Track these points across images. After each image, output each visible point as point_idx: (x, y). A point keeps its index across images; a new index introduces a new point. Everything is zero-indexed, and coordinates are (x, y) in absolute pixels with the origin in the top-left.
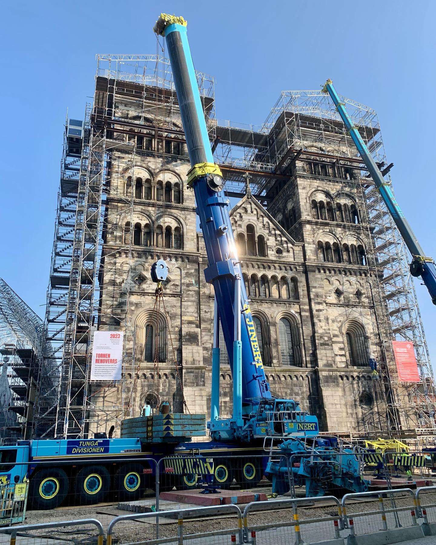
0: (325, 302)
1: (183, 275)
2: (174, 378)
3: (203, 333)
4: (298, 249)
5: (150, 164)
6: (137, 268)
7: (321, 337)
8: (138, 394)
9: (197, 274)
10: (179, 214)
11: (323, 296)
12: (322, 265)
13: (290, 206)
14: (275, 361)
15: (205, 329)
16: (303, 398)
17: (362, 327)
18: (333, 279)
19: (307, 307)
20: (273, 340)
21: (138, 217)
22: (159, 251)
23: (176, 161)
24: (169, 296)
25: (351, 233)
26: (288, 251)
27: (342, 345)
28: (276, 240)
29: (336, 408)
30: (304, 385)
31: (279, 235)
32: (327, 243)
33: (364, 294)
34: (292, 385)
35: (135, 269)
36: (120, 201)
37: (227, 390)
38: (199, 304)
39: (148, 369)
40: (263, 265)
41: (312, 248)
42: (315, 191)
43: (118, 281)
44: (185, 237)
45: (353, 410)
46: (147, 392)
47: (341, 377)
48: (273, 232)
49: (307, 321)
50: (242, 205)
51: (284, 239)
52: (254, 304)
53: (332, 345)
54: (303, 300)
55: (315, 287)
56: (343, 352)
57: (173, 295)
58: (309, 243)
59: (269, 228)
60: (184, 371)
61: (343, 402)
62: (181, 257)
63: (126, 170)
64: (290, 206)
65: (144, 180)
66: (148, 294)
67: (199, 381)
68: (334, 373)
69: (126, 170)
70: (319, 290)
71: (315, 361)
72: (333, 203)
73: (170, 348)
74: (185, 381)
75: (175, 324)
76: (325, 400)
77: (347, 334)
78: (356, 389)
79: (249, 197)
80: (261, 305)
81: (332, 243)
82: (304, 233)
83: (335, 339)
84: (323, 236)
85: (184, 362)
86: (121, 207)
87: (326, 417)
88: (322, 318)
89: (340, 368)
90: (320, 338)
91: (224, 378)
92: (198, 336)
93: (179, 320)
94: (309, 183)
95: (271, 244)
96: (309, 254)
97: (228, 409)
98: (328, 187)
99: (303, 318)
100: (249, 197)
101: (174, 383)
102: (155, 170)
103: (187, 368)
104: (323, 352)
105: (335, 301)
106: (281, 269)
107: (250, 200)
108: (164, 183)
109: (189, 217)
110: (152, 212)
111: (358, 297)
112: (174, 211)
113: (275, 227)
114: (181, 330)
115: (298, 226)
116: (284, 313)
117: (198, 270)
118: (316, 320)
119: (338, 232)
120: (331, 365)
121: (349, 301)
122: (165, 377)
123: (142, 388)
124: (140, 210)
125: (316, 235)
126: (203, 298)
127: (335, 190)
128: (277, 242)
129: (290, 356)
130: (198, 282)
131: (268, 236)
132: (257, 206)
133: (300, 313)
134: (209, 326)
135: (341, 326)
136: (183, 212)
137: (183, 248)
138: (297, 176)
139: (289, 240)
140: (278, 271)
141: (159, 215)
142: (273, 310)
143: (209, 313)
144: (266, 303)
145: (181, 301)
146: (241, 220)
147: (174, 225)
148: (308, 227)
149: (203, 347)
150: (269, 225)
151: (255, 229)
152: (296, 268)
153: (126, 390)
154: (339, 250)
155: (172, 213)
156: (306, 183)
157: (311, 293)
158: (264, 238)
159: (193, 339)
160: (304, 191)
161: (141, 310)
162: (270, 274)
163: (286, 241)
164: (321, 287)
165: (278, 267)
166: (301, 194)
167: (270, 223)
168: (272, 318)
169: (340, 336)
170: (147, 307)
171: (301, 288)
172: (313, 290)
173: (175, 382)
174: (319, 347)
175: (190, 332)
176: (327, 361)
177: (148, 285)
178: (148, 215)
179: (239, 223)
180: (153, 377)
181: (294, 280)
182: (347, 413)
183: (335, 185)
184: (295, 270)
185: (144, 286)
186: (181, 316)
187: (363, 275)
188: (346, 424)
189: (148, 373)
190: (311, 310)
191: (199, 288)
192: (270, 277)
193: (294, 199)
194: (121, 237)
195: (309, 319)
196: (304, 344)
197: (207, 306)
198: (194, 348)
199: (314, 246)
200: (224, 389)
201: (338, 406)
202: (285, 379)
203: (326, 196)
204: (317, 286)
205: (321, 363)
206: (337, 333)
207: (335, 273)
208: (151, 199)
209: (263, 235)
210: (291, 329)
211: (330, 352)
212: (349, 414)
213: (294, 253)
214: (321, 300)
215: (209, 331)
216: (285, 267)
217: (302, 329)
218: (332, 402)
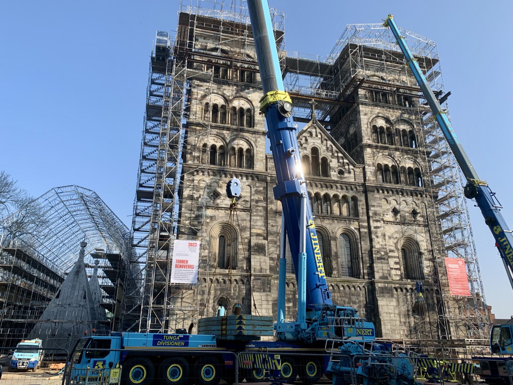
0: (383, 220)
1: (253, 192)
2: (243, 283)
3: (270, 245)
4: (358, 171)
5: (225, 92)
6: (212, 185)
7: (378, 252)
8: (212, 297)
9: (265, 191)
10: (250, 137)
11: (381, 214)
12: (381, 186)
13: (352, 131)
14: (335, 272)
15: (272, 241)
16: (360, 307)
17: (417, 244)
18: (390, 199)
19: (366, 224)
20: (333, 253)
21: (213, 140)
22: (232, 170)
23: (248, 89)
24: (240, 211)
25: (409, 156)
26: (350, 172)
27: (397, 260)
28: (338, 162)
29: (390, 317)
30: (361, 295)
31: (342, 157)
33: (419, 213)
34: (350, 294)
35: (210, 186)
36: (198, 125)
37: (291, 297)
38: (266, 219)
39: (220, 275)
40: (326, 185)
41: (372, 170)
42: (376, 117)
43: (195, 196)
44: (255, 158)
45: (406, 319)
46: (220, 295)
47: (396, 289)
48: (336, 155)
49: (365, 237)
50: (307, 129)
51: (346, 161)
52: (317, 220)
53: (388, 260)
54: (363, 218)
55: (374, 206)
56: (398, 266)
57: (244, 210)
58: (369, 165)
59: (332, 151)
60: (252, 278)
61: (397, 311)
62: (251, 176)
63: (204, 97)
64: (352, 131)
65: (219, 106)
66: (221, 208)
67: (265, 287)
68: (389, 285)
69: (204, 97)
70: (377, 209)
71: (371, 273)
72: (393, 128)
73: (241, 257)
74: (254, 287)
75: (245, 236)
76: (380, 309)
77: (402, 249)
78: (409, 300)
79: (315, 122)
80: (323, 221)
81: (390, 166)
82: (365, 156)
83: (391, 254)
84: (382, 159)
85: (252, 270)
86: (199, 130)
87: (381, 324)
88: (379, 234)
89: (395, 280)
90: (377, 253)
91: (288, 286)
92: (265, 247)
93: (249, 233)
94: (370, 110)
95: (334, 166)
96: (368, 174)
97: (291, 313)
98: (388, 114)
99: (362, 234)
100: (315, 122)
101: (244, 288)
102: (229, 96)
104: (379, 265)
105: (392, 219)
106: (342, 189)
107: (315, 124)
108: (237, 109)
109: (259, 139)
111: (413, 216)
112: (245, 134)
113: (337, 150)
114: (250, 242)
115: (359, 150)
116: (344, 229)
117: (266, 188)
118: (373, 236)
119: (396, 155)
120: (386, 278)
121: (405, 220)
122: (235, 283)
123: (215, 292)
124: (216, 133)
125: (376, 158)
126: (270, 214)
127: (394, 116)
128: (339, 164)
129: (348, 268)
130: (266, 199)
131: (331, 158)
132: (321, 130)
133: (359, 230)
134: (275, 239)
135: (397, 242)
136: (254, 136)
137: (253, 168)
138: (359, 103)
139: (350, 162)
140: (340, 190)
141: (233, 137)
142: (334, 226)
143: (275, 227)
144: (328, 219)
145: (251, 216)
146: (307, 143)
148: (369, 150)
149: (270, 258)
150: (332, 148)
151: (319, 152)
152: (356, 188)
153: (201, 293)
154: (397, 172)
156: (367, 109)
157: (370, 211)
158: (327, 160)
159: (261, 249)
160: (366, 117)
161: (215, 222)
162: (332, 193)
163: (347, 163)
164: (379, 206)
165: (339, 187)
166: (363, 119)
167: (334, 146)
168: (333, 233)
169: (396, 252)
170: (221, 220)
171: (361, 207)
172: (372, 208)
173: (244, 287)
174: (375, 261)
175: (258, 243)
176: (383, 273)
177: (221, 201)
178: (222, 138)
179: (304, 145)
180: (225, 282)
181: (354, 199)
182: (401, 322)
183: (394, 112)
184: (355, 190)
185: (218, 201)
186: (250, 229)
187: (419, 196)
188: (399, 331)
189: (221, 279)
190: (369, 227)
191: (267, 204)
192: (332, 196)
194: (198, 157)
195: (367, 235)
196: (362, 258)
197: (273, 220)
198: (262, 258)
199: (374, 168)
200: (288, 296)
201: (392, 315)
202: (344, 288)
203: (386, 122)
204: (376, 205)
205: (378, 275)
206: (393, 248)
207: (393, 193)
208: (225, 123)
209: (326, 157)
210: (350, 244)
211: (386, 265)
212: (402, 323)
213: (355, 174)
214: (379, 218)
215: (275, 243)
216: (346, 187)
217: (361, 244)
218: (387, 311)
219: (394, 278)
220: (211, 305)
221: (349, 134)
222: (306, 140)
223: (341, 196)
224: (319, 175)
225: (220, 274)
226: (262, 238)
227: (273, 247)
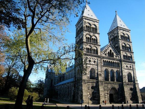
1: (98, 61)
4: (120, 56)
5: (91, 34)
15: (102, 73)
18: (126, 63)
32: (125, 55)
38: (101, 67)
55: (123, 65)
57: (96, 65)
67: (102, 84)
103: (100, 81)
114: (98, 73)
117: (101, 60)
118: (123, 72)
148: (122, 51)
162: (114, 61)
170: (91, 67)
181: (119, 63)
185: (91, 63)
190: (122, 70)
192: (114, 62)
215: (103, 73)
219: (127, 82)
222: (109, 48)
223: (116, 62)
225: (92, 81)
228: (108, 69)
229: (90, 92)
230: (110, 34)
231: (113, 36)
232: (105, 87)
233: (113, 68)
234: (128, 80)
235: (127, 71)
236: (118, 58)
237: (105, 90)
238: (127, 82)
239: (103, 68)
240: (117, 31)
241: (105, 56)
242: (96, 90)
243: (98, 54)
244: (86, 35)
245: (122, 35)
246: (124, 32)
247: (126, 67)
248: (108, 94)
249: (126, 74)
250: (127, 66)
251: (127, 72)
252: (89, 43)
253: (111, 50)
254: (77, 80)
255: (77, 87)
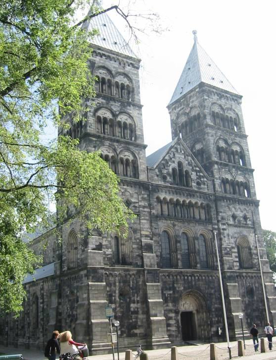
4: (210, 183)
5: (112, 107)
8: (117, 288)
14: (198, 265)
17: (248, 242)
23: (130, 106)
28: (197, 175)
32: (227, 179)
38: (151, 222)
44: (139, 168)
47: (237, 276)
51: (201, 174)
55: (221, 212)
58: (217, 179)
60: (146, 272)
70: (224, 214)
85: (145, 265)
86: (96, 141)
91: (169, 277)
96: (217, 186)
102: (116, 112)
103: (148, 270)
106: (200, 198)
109: (141, 152)
110: (116, 146)
112: (131, 147)
117: (149, 196)
118: (222, 237)
125: (220, 173)
126: (153, 218)
130: (150, 205)
133: (212, 231)
134: (158, 239)
141: (121, 149)
147: (131, 158)
148: (216, 166)
155: (129, 148)
159: (149, 248)
162: (193, 201)
167: (193, 162)
172: (220, 214)
179: (173, 159)
187: (248, 204)
190: (219, 229)
192: (194, 203)
193: (204, 143)
204: (223, 211)
206: (234, 245)
207: (233, 201)
220: (117, 295)
221: (195, 149)
222: (174, 155)
224: (184, 186)
225: (122, 269)
226: (149, 238)
227: (157, 246)
228: (174, 225)
229: (118, 309)
230: (175, 108)
231: (185, 114)
232: (167, 289)
233: (189, 221)
234: (240, 261)
235: (235, 233)
236: (206, 191)
237: (166, 300)
238: (236, 268)
239: (158, 225)
240: (199, 100)
241: (162, 183)
242: (138, 302)
243: (138, 178)
244: (96, 110)
245: (217, 113)
246: (223, 102)
247: (231, 219)
248: (177, 312)
249: (232, 240)
250: (234, 217)
251: (236, 235)
252: (108, 139)
253: (180, 164)
254: (69, 269)
255: (67, 296)
